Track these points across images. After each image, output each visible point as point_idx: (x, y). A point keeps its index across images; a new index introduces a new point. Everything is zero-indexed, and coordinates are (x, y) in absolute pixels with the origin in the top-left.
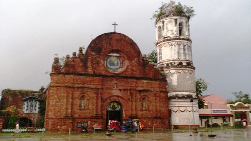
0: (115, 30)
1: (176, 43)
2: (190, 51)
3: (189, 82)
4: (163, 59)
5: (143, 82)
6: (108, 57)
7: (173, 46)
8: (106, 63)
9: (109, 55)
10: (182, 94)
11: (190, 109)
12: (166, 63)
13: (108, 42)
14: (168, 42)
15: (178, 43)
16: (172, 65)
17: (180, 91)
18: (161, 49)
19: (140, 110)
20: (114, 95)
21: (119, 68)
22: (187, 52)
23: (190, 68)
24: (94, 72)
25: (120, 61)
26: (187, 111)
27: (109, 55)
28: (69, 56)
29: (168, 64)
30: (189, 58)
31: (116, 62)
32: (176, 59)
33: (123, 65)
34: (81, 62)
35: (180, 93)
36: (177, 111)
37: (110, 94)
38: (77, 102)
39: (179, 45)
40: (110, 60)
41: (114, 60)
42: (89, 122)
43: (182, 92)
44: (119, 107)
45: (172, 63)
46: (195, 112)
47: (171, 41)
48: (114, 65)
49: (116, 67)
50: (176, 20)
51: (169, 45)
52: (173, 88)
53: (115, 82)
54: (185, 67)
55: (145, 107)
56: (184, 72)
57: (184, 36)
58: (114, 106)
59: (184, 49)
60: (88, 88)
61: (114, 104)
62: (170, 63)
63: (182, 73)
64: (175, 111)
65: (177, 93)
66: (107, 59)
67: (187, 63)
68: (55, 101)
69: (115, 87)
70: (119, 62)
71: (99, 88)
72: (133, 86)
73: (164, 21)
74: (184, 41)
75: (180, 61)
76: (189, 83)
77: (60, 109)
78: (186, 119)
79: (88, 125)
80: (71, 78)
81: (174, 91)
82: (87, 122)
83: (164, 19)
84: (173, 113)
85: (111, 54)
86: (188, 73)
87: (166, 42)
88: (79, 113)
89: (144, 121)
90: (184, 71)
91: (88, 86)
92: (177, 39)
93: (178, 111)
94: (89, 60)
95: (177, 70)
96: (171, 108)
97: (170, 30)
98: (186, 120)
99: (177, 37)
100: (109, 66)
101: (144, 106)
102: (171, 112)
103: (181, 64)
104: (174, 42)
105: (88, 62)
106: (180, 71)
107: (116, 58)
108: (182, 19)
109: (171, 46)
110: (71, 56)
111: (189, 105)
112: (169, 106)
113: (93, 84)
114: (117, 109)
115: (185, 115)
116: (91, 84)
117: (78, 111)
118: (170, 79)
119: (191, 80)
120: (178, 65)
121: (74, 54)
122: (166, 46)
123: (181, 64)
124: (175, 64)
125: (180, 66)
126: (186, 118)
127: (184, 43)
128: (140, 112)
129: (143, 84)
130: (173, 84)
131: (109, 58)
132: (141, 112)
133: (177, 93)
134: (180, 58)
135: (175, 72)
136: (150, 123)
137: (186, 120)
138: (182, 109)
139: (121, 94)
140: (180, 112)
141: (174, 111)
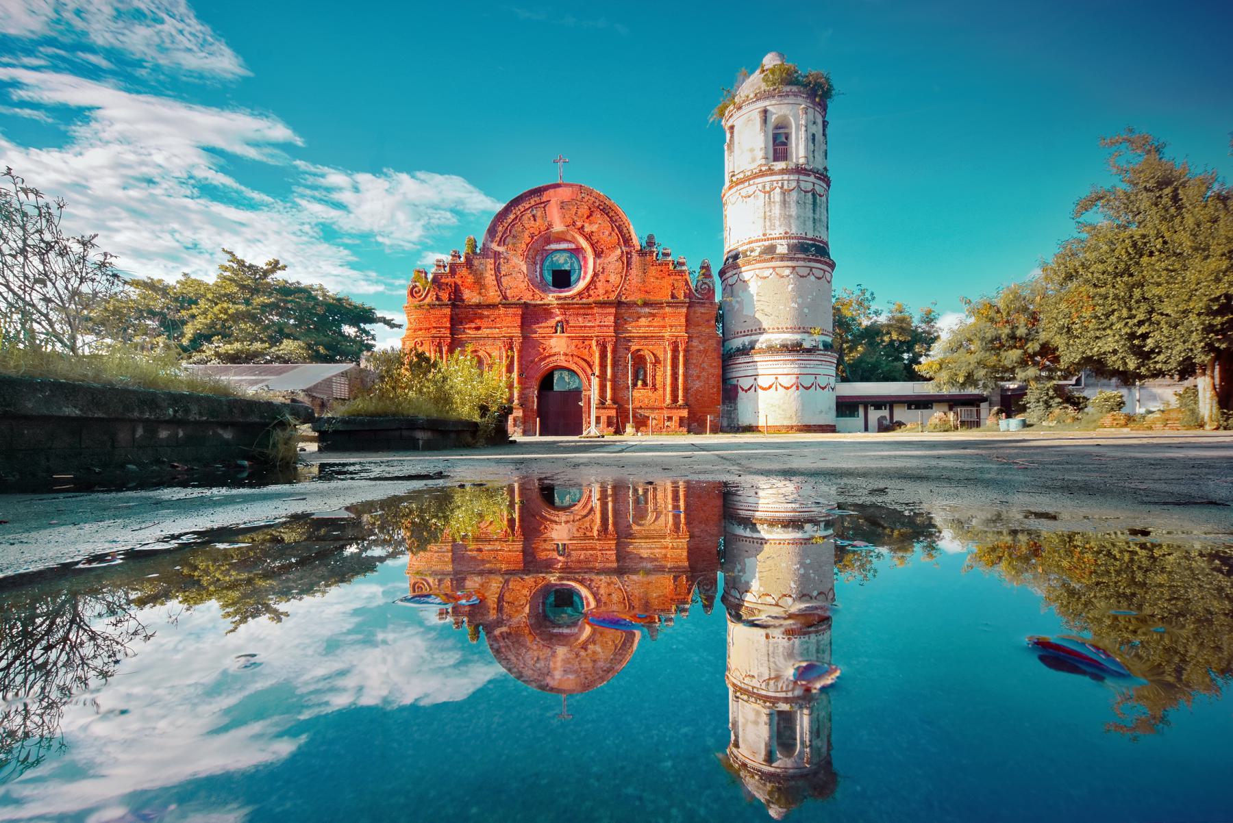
1: (760, 187)
8: (538, 270)
20: (553, 351)
23: (798, 259)
26: (779, 386)
36: (749, 389)
41: (562, 261)
47: (747, 184)
54: (782, 258)
64: (746, 388)
74: (786, 177)
75: (767, 243)
85: (554, 246)
92: (762, 174)
93: (753, 389)
102: (737, 393)
103: (771, 250)
106: (767, 273)
107: (566, 255)
112: (734, 375)
120: (762, 253)
123: (771, 250)
127: (786, 183)
141: (743, 390)
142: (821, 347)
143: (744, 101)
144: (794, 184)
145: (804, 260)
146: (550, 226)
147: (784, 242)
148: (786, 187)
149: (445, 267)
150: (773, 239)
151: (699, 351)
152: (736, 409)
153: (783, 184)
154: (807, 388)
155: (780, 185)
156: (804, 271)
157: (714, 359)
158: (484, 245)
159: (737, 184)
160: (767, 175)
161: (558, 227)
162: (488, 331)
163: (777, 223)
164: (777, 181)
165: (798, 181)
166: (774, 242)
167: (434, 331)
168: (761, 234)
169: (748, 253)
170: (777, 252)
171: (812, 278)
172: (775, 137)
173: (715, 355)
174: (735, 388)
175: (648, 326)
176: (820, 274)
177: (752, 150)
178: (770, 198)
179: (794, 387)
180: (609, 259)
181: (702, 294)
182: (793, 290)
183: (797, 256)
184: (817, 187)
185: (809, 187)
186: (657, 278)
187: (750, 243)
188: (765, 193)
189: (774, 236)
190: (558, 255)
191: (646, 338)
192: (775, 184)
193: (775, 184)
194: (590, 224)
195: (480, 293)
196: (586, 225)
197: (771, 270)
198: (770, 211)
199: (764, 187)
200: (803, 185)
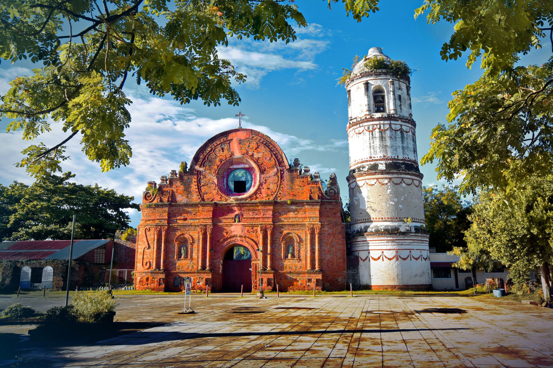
1: (366, 128)
6: (229, 172)
7: (362, 134)
8: (225, 181)
9: (231, 167)
14: (354, 127)
15: (369, 128)
16: (360, 171)
20: (233, 234)
23: (393, 173)
26: (384, 258)
31: (245, 177)
32: (366, 159)
34: (181, 185)
36: (366, 259)
41: (240, 175)
45: (360, 167)
47: (358, 126)
50: (367, 84)
54: (382, 172)
61: (239, 249)
64: (364, 258)
68: (143, 247)
71: (207, 225)
72: (266, 218)
74: (382, 122)
75: (372, 163)
90: (380, 180)
92: (367, 120)
102: (359, 261)
106: (373, 182)
107: (243, 171)
111: (389, 247)
116: (196, 219)
118: (357, 198)
120: (369, 169)
125: (371, 171)
127: (382, 126)
130: (360, 208)
131: (231, 172)
141: (362, 260)
142: (413, 230)
143: (354, 77)
144: (387, 126)
145: (397, 173)
146: (232, 154)
147: (383, 162)
148: (382, 128)
149: (166, 180)
151: (329, 234)
152: (358, 273)
153: (380, 126)
154: (404, 259)
155: (378, 127)
156: (398, 181)
157: (339, 239)
159: (353, 126)
160: (370, 121)
161: (237, 155)
162: (191, 221)
163: (378, 150)
164: (377, 125)
165: (390, 124)
166: (377, 162)
167: (157, 222)
169: (361, 169)
170: (379, 168)
171: (404, 185)
172: (375, 98)
173: (340, 236)
174: (357, 258)
175: (295, 218)
176: (409, 182)
177: (361, 105)
178: (372, 135)
179: (395, 258)
180: (269, 174)
181: (330, 196)
182: (390, 193)
183: (391, 171)
184: (404, 128)
185: (398, 127)
186: (301, 186)
187: (363, 162)
188: (369, 131)
189: (377, 158)
191: (293, 225)
192: (375, 126)
193: (375, 126)
194: (258, 153)
195: (187, 197)
196: (255, 153)
197: (376, 180)
198: (373, 143)
199: (369, 128)
200: (393, 126)
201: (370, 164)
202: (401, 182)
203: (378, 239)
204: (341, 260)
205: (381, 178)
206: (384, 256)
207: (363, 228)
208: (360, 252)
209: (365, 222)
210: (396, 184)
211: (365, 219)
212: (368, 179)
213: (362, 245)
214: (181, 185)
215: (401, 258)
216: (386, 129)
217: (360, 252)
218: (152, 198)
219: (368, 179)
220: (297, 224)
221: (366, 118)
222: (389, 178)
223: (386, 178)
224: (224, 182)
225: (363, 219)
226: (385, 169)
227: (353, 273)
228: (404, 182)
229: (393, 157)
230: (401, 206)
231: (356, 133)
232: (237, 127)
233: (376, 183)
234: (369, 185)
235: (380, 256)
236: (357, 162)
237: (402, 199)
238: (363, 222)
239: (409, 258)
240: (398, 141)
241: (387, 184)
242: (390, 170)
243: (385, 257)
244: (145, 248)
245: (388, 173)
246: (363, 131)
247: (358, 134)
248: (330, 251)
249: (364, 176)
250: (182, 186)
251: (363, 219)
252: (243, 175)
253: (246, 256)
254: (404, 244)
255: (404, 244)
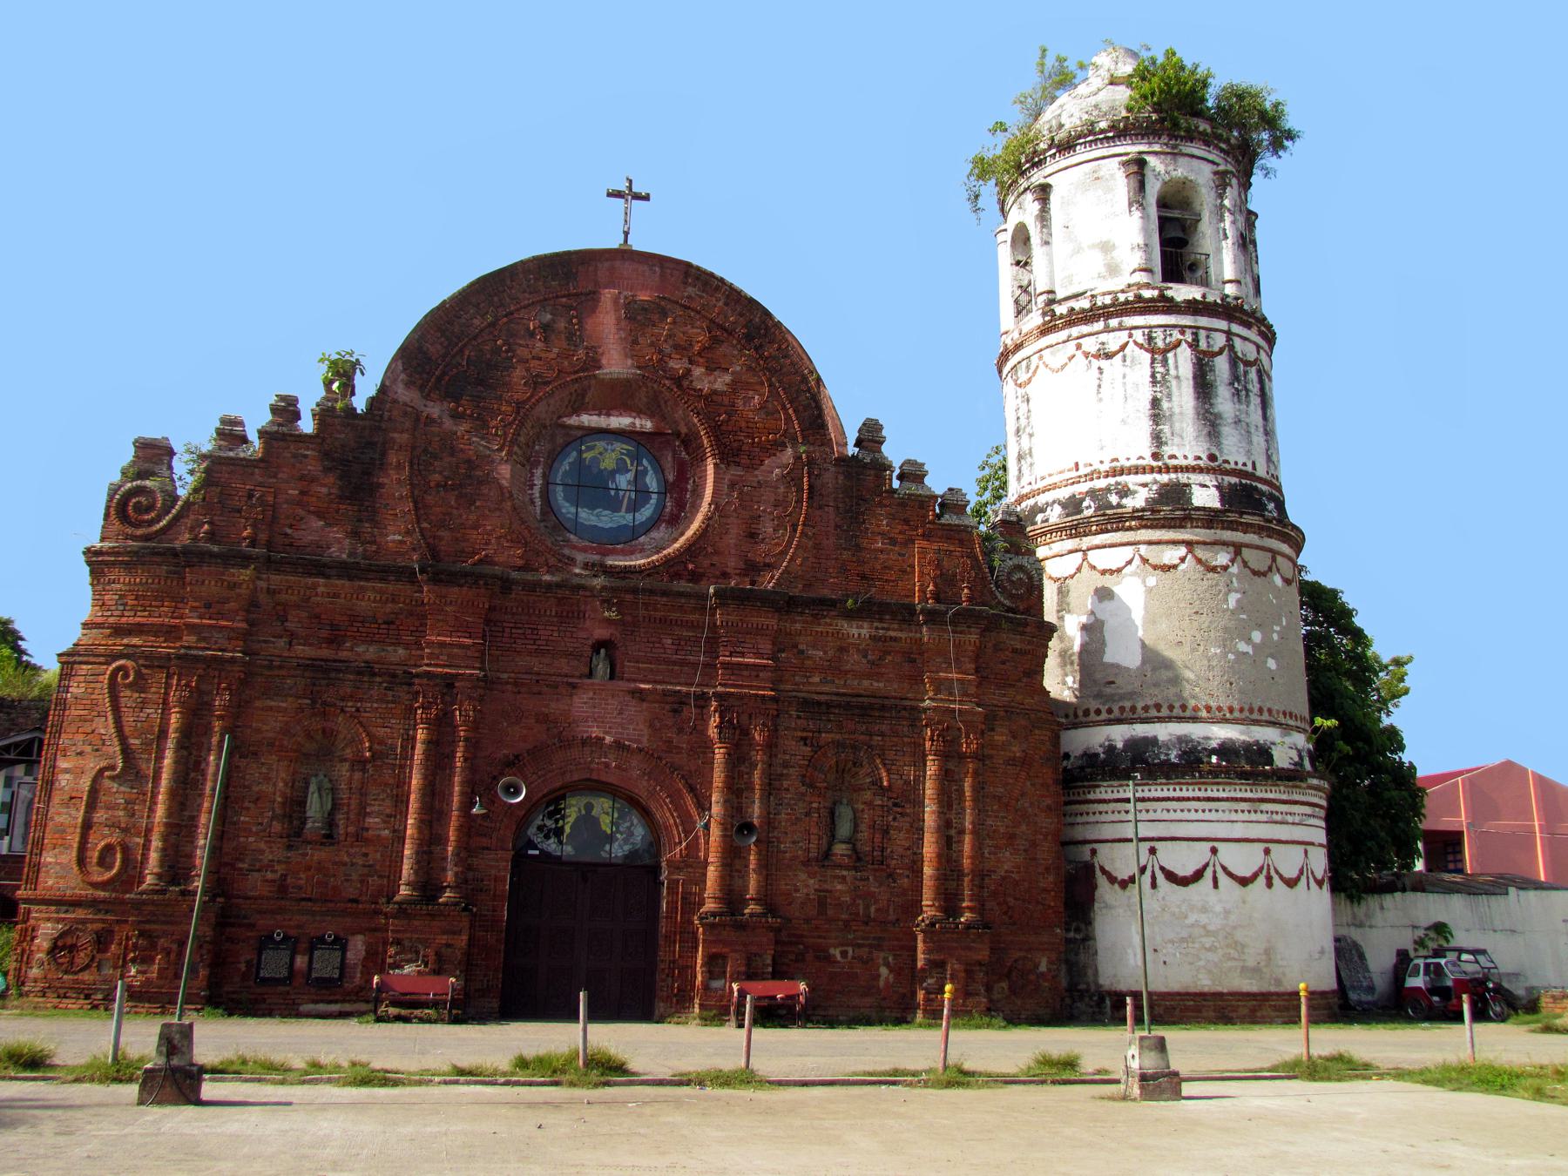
0: (626, 234)
1: (1138, 336)
2: (1255, 400)
3: (1249, 641)
4: (1040, 470)
5: (837, 634)
6: (560, 440)
8: (538, 482)
9: (573, 421)
10: (1181, 740)
11: (1243, 860)
12: (1064, 493)
13: (561, 324)
14: (1075, 331)
15: (1150, 339)
16: (1103, 506)
17: (1165, 712)
18: (1029, 389)
19: (807, 863)
21: (653, 524)
22: (1224, 402)
23: (1246, 528)
24: (434, 552)
25: (660, 470)
26: (1221, 875)
27: (573, 421)
28: (238, 422)
29: (1072, 505)
30: (1249, 453)
31: (630, 476)
32: (1134, 462)
33: (680, 505)
34: (327, 470)
35: (1164, 732)
37: (543, 719)
38: (267, 779)
39: (1161, 354)
40: (580, 460)
41: (608, 463)
42: (357, 947)
43: (1180, 719)
44: (632, 834)
45: (1108, 490)
46: (1291, 883)
47: (1099, 325)
48: (614, 505)
49: (624, 518)
51: (1086, 355)
52: (1108, 690)
53: (601, 633)
55: (850, 841)
56: (1199, 561)
57: (1205, 282)
58: (588, 821)
59: (1203, 386)
60: (369, 670)
61: (589, 807)
62: (1092, 493)
63: (1180, 568)
64: (1123, 875)
65: (1141, 730)
66: (553, 458)
67: (1226, 494)
68: (93, 764)
69: (602, 668)
70: (652, 482)
73: (1049, 180)
74: (1203, 321)
75: (1164, 478)
76: (1243, 647)
77: (125, 830)
78: (1208, 942)
79: (343, 965)
80: (233, 586)
81: (1116, 713)
82: (341, 943)
83: (1048, 170)
84: (1105, 890)
85: (588, 420)
86: (1234, 569)
87: (1063, 335)
88: (280, 869)
89: (836, 952)
90: (1200, 552)
91: (369, 652)
94: (393, 458)
95: (1143, 549)
96: (1094, 852)
97: (1093, 246)
98: (1211, 949)
99: (1147, 294)
100: (567, 509)
101: (844, 829)
102: (1094, 887)
103: (1174, 495)
104: (1120, 328)
105: (383, 466)
106: (1171, 555)
107: (620, 447)
108: (1182, 160)
109: (1096, 363)
110: (256, 420)
111: (1238, 831)
112: (1080, 833)
113: (407, 646)
114: (618, 850)
115: (1204, 910)
117: (272, 853)
119: (1259, 626)
120: (1152, 506)
121: (286, 409)
122: (1063, 367)
123: (1174, 495)
124: (1124, 501)
126: (1208, 933)
127: (1202, 334)
128: (803, 876)
129: (842, 649)
132: (811, 875)
133: (1141, 730)
134: (1167, 450)
135: (1129, 562)
136: (884, 971)
137: (1211, 949)
138: (1184, 860)
139: (646, 731)
140: (1160, 877)
141: (1112, 879)
144: (1219, 340)
145: (1259, 530)
148: (1203, 345)
150: (1177, 469)
151: (1012, 761)
152: (1088, 938)
154: (1291, 883)
158: (383, 389)
160: (1156, 311)
161: (616, 364)
162: (369, 652)
165: (1229, 333)
166: (1183, 478)
167: (189, 639)
168: (1147, 454)
169: (1114, 499)
171: (1278, 580)
175: (869, 676)
177: (1106, 247)
179: (1261, 879)
180: (759, 474)
181: (1011, 597)
182: (1240, 607)
186: (893, 542)
187: (1114, 472)
189: (1184, 463)
190: (600, 445)
193: (1176, 335)
194: (710, 370)
195: (355, 534)
198: (1169, 396)
199: (1150, 339)
200: (1237, 342)
201: (1156, 482)
202: (1270, 569)
203: (1198, 794)
204: (1051, 878)
205: (1205, 543)
206: (1217, 864)
207: (1120, 745)
208: (1103, 849)
209: (1131, 721)
210: (1256, 573)
211: (1133, 709)
212: (1150, 543)
213: (1116, 817)
214: (327, 470)
215: (1281, 877)
216: (1216, 349)
217: (1103, 849)
218: (151, 523)
219: (1150, 543)
220: (883, 708)
221: (1139, 298)
222: (1233, 544)
223: (1225, 544)
224: (532, 486)
225: (1122, 709)
226: (1217, 505)
227: (1072, 935)
228: (1278, 570)
229: (1240, 466)
230: (1272, 664)
231: (1086, 355)
232: (614, 242)
233: (1183, 560)
234: (1155, 567)
235: (1207, 865)
236: (1083, 471)
237: (1275, 637)
238: (1119, 721)
239: (1304, 878)
240: (1252, 407)
241: (1225, 568)
242: (1241, 514)
243: (1224, 868)
244: (101, 771)
245: (1232, 526)
246: (1123, 348)
247: (1093, 356)
248: (1012, 837)
249: (1130, 529)
250: (330, 479)
251: (1122, 709)
252: (620, 462)
253: (626, 841)
254: (1290, 819)
255: (1290, 819)
